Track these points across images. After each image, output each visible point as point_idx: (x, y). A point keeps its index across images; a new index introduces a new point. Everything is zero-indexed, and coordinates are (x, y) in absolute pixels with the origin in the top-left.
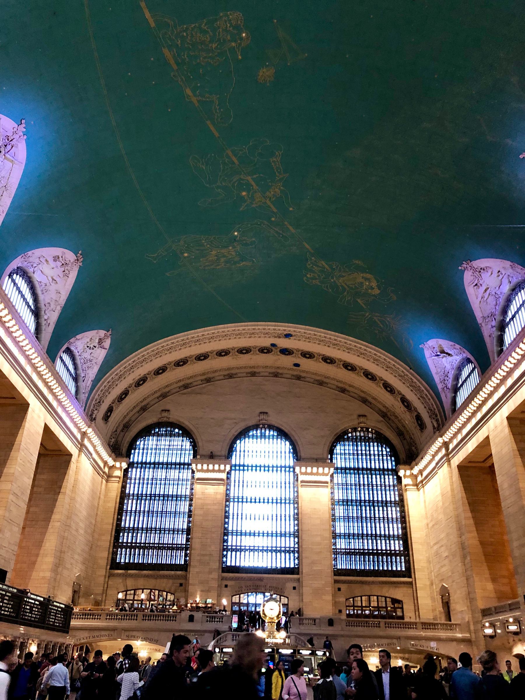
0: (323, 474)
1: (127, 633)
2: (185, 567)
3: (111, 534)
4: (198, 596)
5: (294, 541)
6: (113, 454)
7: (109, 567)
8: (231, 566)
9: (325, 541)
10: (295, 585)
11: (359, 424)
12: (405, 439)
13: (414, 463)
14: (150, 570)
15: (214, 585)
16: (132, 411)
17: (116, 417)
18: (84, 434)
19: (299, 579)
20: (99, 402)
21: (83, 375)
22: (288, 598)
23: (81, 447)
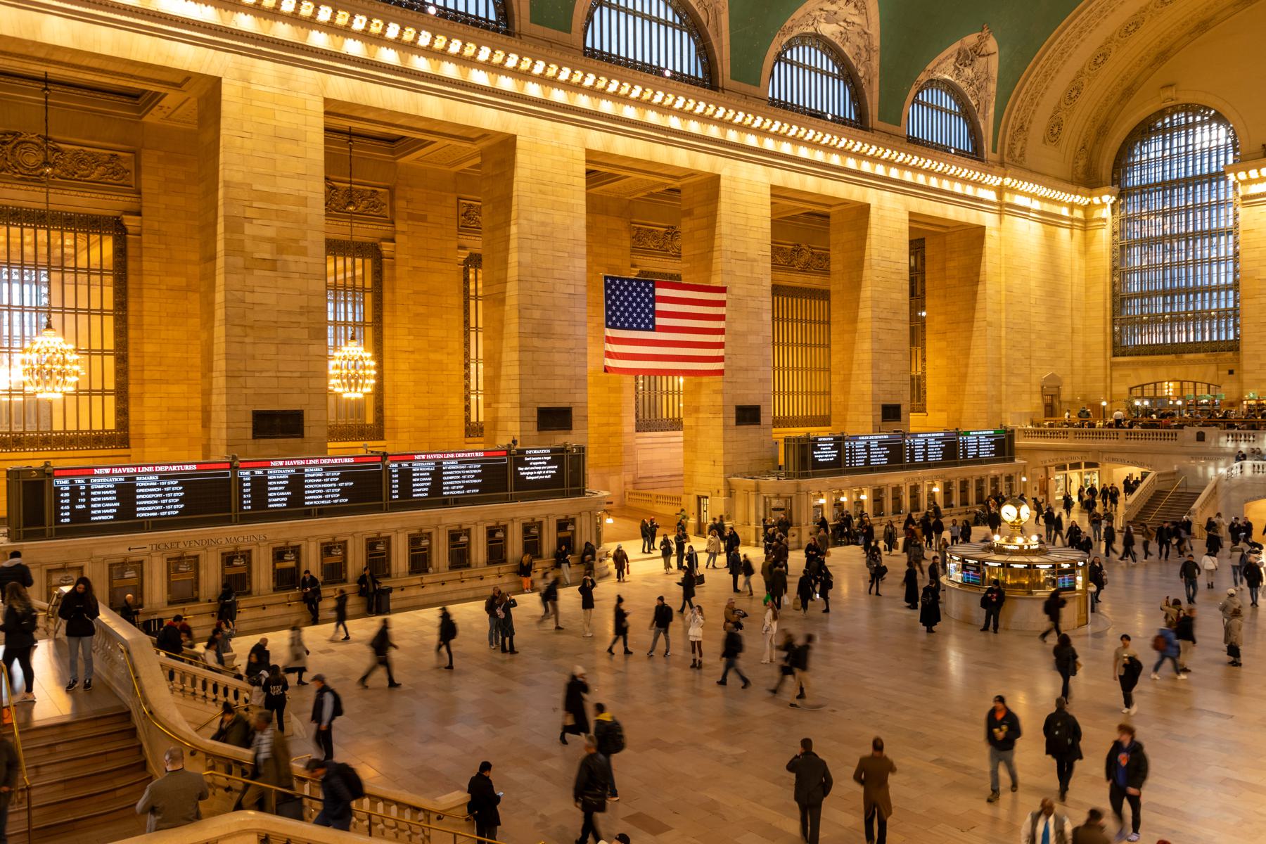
1: (1106, 456)
2: (1234, 347)
6: (1081, 189)
7: (1109, 354)
17: (1076, 126)
18: (1000, 190)
20: (1021, 127)
21: (974, 103)
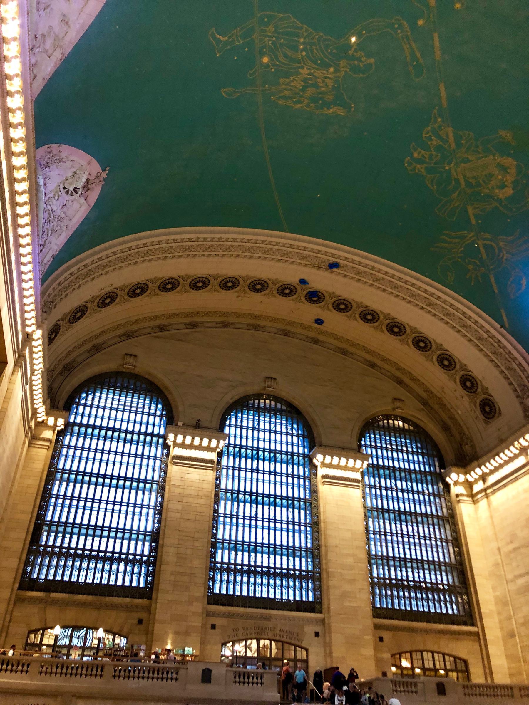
0: (354, 469)
2: (147, 593)
3: (28, 531)
4: (169, 642)
5: (313, 562)
6: (48, 401)
7: (17, 585)
8: (220, 594)
9: (359, 564)
10: (318, 629)
11: (394, 409)
12: (452, 436)
13: (476, 463)
14: (89, 594)
15: (196, 624)
16: (80, 346)
19: (324, 619)
22: (307, 650)
23: (20, 358)
